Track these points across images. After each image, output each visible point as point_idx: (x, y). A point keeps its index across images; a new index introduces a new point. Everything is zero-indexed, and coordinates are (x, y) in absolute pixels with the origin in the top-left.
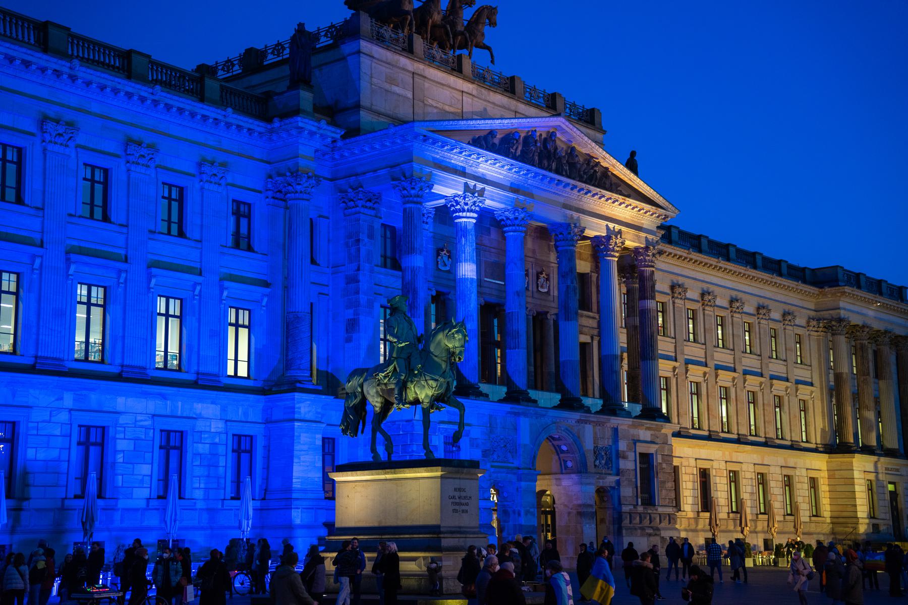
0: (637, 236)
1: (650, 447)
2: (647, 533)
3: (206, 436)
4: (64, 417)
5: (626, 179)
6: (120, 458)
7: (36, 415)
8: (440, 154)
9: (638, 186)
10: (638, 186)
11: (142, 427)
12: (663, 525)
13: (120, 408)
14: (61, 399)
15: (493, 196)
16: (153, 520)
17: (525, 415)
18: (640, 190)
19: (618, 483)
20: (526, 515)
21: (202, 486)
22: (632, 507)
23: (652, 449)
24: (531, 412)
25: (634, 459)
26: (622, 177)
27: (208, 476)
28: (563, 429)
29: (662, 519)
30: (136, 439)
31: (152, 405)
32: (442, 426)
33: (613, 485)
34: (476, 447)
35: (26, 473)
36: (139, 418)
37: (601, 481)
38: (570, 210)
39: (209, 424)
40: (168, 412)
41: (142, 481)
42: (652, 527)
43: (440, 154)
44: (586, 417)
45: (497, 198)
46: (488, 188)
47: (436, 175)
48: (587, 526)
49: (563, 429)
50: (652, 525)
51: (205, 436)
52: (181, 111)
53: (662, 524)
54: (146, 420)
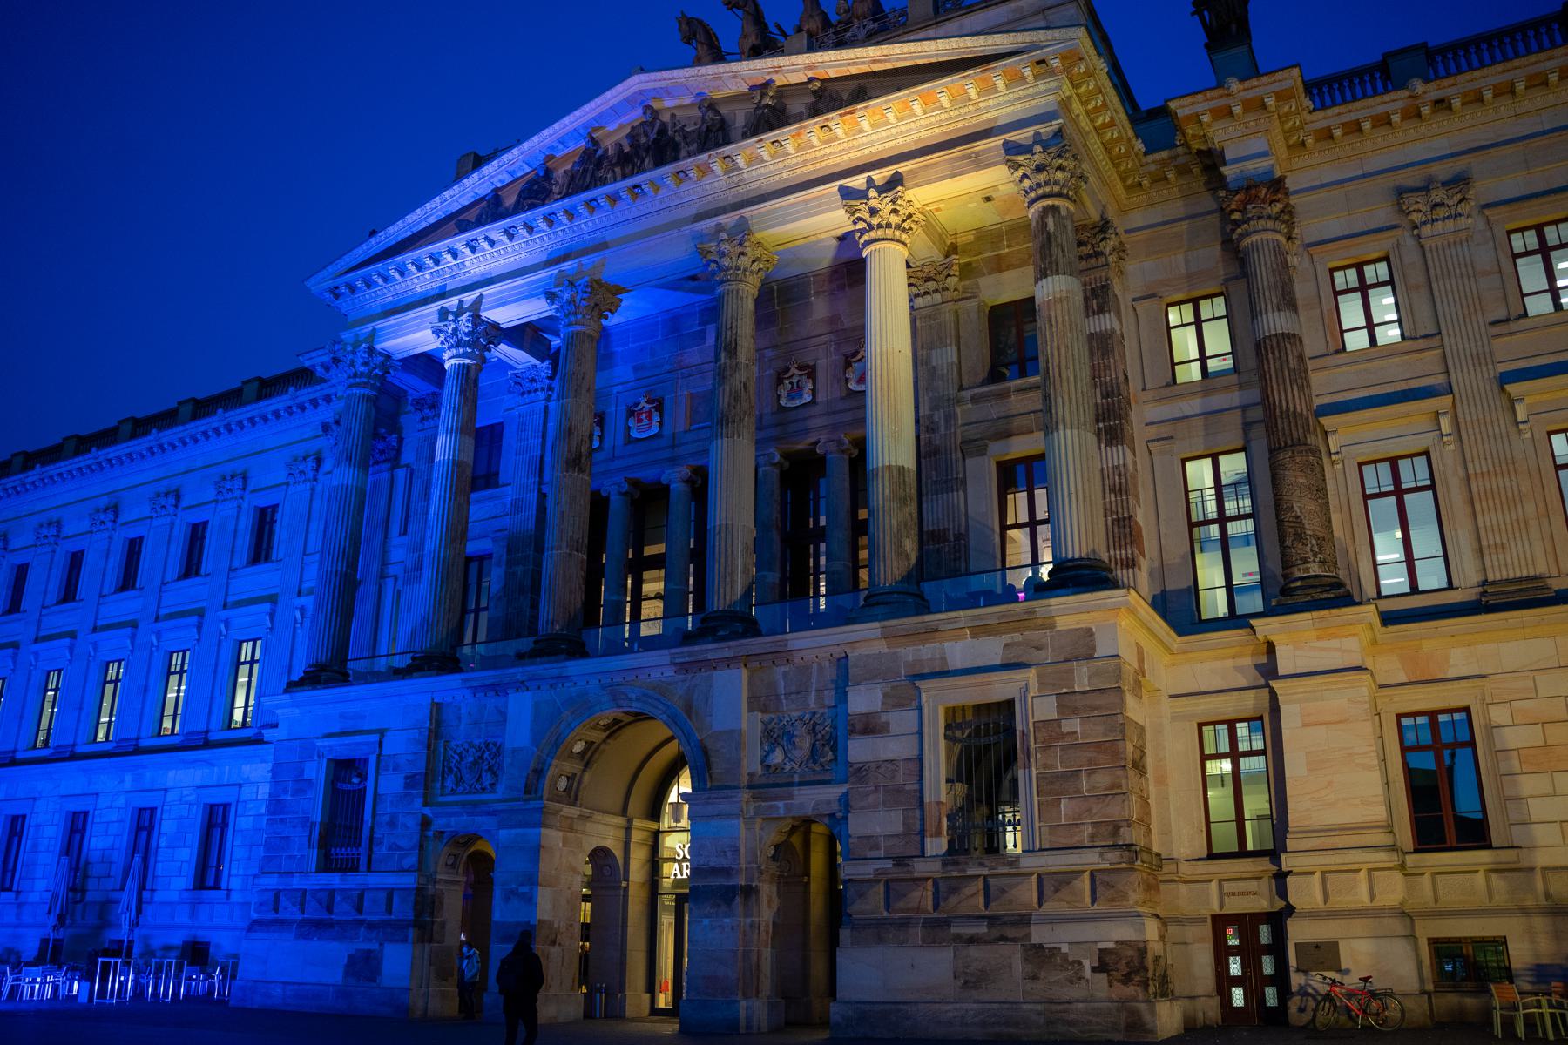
0: (963, 158)
1: (990, 683)
2: (958, 938)
3: (252, 805)
4: (121, 801)
5: (865, 69)
6: (163, 843)
7: (103, 802)
8: (386, 295)
9: (905, 59)
10: (905, 59)
11: (186, 803)
12: (1050, 907)
13: (170, 784)
14: (122, 781)
15: (501, 298)
16: (183, 917)
17: (520, 686)
18: (920, 62)
19: (845, 802)
20: (507, 899)
21: (241, 872)
22: (889, 864)
23: (1000, 687)
24: (519, 677)
25: (915, 729)
26: (854, 70)
27: (249, 859)
28: (634, 696)
29: (1048, 890)
30: (181, 818)
31: (197, 775)
32: (319, 743)
33: (835, 807)
34: (393, 770)
35: (87, 863)
36: (185, 793)
37: (781, 804)
38: (716, 216)
39: (255, 790)
40: (215, 783)
41: (180, 869)
42: (993, 920)
43: (386, 295)
44: (690, 654)
45: (509, 296)
46: (486, 291)
47: (382, 329)
48: (706, 921)
49: (634, 696)
50: (995, 909)
51: (250, 805)
52: (252, 421)
53: (1045, 905)
54: (191, 794)
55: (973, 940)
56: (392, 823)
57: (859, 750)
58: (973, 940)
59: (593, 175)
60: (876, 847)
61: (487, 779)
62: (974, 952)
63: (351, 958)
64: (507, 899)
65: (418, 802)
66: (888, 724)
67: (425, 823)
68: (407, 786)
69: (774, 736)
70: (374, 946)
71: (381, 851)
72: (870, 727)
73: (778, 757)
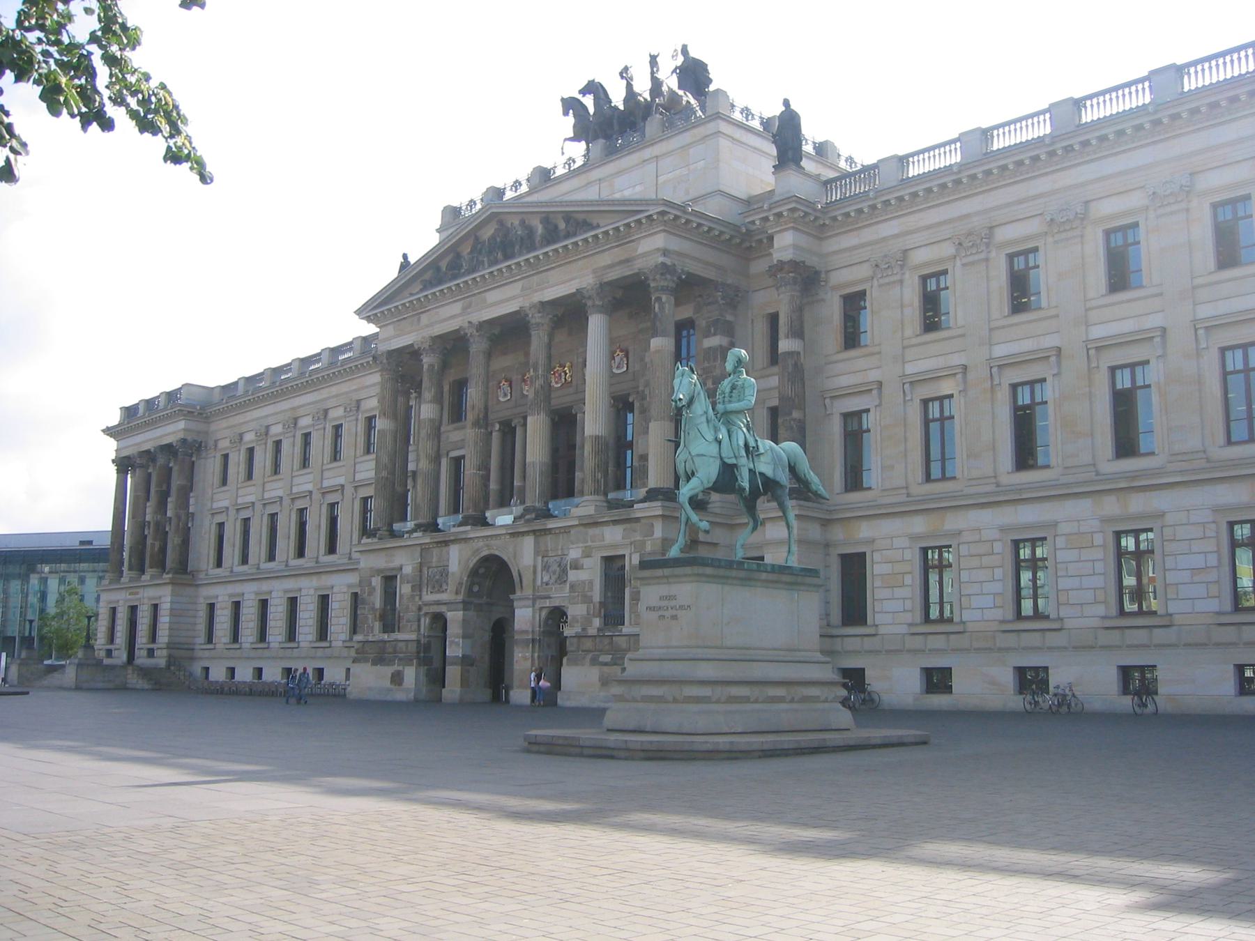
20: (451, 645)
55: (606, 664)
56: (407, 608)
57: (573, 576)
58: (606, 664)
59: (477, 260)
60: (577, 622)
61: (444, 587)
62: (606, 669)
63: (392, 674)
64: (451, 645)
65: (417, 598)
66: (583, 565)
67: (420, 609)
68: (413, 591)
69: (546, 568)
70: (400, 668)
71: (403, 623)
72: (576, 566)
73: (545, 579)
